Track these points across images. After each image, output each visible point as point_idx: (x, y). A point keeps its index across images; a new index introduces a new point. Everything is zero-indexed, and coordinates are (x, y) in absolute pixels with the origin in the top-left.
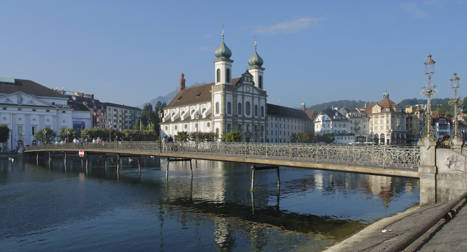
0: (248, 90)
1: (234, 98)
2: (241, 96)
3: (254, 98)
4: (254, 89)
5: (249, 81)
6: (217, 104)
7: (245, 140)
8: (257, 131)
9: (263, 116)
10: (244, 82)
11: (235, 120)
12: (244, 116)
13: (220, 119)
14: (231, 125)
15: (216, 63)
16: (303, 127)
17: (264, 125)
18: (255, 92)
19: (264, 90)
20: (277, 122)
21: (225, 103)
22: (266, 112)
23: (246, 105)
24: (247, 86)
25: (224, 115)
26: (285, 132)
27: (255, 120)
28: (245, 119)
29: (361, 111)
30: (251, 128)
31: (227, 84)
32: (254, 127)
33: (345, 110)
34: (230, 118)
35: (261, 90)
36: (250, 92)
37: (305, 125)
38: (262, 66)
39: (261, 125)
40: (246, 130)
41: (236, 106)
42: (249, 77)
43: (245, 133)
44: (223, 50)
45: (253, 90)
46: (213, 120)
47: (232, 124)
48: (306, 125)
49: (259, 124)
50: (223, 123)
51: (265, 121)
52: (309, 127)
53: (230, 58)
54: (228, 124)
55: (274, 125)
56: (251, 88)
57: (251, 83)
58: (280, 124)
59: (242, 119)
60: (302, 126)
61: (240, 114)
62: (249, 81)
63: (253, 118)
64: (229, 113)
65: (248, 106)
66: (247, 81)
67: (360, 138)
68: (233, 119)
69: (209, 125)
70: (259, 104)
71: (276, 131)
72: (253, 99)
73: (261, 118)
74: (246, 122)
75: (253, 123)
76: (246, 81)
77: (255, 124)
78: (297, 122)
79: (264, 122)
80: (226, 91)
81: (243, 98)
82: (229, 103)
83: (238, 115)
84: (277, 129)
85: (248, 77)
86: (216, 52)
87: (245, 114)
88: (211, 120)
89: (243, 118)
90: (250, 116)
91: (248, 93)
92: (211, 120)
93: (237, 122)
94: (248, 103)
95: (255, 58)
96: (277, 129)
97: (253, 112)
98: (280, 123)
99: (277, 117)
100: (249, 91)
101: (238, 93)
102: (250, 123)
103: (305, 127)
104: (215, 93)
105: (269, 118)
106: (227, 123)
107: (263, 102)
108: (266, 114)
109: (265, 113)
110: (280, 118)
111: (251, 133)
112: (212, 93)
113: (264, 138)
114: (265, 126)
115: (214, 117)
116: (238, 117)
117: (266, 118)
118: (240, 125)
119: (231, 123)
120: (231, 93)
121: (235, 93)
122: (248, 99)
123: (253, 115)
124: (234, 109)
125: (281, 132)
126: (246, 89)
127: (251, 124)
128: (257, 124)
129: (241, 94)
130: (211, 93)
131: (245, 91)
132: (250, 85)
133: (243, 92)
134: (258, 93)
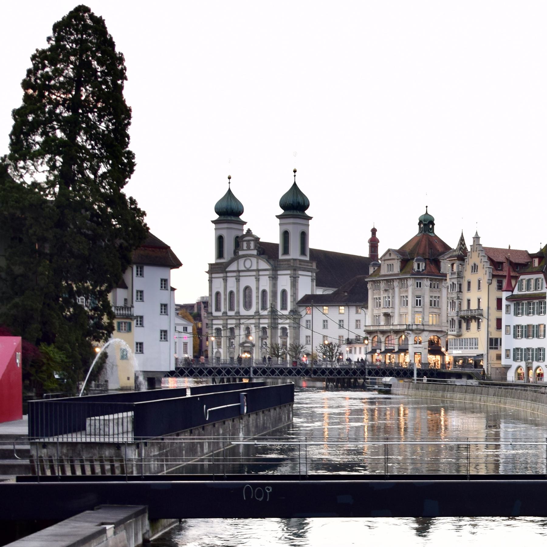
2: (234, 279)
4: (259, 260)
12: (238, 312)
14: (220, 329)
17: (287, 326)
36: (252, 268)
40: (243, 338)
43: (241, 342)
45: (257, 262)
56: (254, 260)
61: (231, 309)
66: (249, 248)
72: (258, 280)
75: (257, 326)
82: (218, 294)
85: (249, 241)
89: (239, 317)
90: (252, 312)
91: (248, 270)
97: (257, 303)
100: (250, 268)
101: (229, 274)
106: (212, 328)
114: (289, 327)
127: (253, 326)
128: (266, 326)
131: (242, 268)
133: (239, 271)
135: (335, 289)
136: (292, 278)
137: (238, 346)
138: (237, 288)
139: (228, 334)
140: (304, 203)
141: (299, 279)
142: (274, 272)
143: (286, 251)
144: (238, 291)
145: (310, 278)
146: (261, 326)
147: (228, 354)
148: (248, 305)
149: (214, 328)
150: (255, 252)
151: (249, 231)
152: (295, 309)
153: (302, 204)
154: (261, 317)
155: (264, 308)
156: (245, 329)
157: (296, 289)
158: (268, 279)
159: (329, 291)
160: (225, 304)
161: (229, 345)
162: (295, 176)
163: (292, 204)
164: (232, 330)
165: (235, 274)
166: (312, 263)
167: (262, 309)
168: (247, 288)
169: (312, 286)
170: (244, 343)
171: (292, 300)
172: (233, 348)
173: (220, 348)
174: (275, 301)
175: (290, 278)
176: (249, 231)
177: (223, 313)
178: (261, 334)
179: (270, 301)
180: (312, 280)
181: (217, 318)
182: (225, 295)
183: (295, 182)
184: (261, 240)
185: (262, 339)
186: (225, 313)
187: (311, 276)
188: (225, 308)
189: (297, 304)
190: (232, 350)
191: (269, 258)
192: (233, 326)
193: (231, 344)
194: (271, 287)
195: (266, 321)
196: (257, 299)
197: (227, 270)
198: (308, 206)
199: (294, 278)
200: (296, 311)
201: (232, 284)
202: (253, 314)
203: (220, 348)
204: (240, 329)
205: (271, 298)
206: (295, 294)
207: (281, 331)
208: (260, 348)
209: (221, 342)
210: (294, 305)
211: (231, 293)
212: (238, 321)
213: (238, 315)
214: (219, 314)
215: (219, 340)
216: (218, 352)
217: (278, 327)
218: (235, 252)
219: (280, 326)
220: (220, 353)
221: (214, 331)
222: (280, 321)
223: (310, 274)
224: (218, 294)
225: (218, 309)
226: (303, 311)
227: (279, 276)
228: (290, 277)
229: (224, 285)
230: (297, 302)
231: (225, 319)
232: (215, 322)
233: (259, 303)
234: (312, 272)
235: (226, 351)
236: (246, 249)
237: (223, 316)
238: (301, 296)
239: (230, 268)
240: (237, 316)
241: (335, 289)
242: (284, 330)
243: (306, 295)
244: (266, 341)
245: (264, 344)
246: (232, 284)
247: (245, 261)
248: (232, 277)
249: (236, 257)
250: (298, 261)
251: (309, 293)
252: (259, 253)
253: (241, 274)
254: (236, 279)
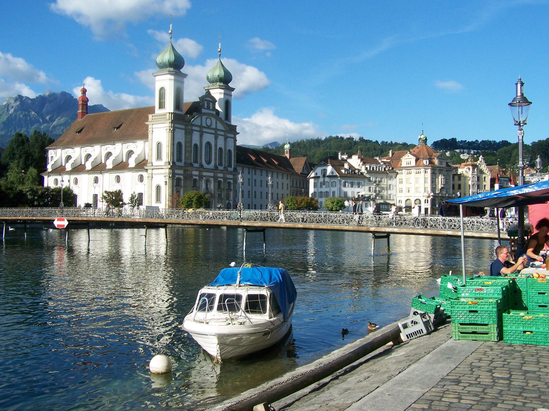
0: (209, 124)
1: (188, 136)
2: (198, 133)
3: (218, 137)
5: (211, 108)
6: (159, 145)
8: (222, 191)
9: (230, 166)
10: (204, 111)
11: (189, 173)
12: (201, 166)
14: (181, 179)
15: (158, 78)
16: (289, 185)
17: (232, 181)
18: (220, 126)
19: (233, 123)
20: (250, 176)
21: (173, 144)
22: (236, 160)
23: (205, 148)
25: (171, 164)
26: (261, 192)
27: (219, 173)
28: (204, 171)
29: (385, 163)
30: (212, 186)
31: (177, 112)
32: (217, 184)
33: (359, 160)
34: (180, 168)
35: (228, 123)
36: (211, 127)
37: (291, 182)
38: (230, 85)
41: (189, 149)
42: (211, 102)
44: (172, 56)
45: (216, 123)
46: (150, 171)
47: (182, 178)
48: (293, 181)
49: (225, 179)
50: (170, 177)
51: (234, 175)
52: (298, 185)
53: (181, 70)
56: (214, 120)
58: (255, 180)
59: (200, 171)
60: (287, 184)
61: (196, 162)
62: (211, 108)
64: (179, 160)
65: (208, 150)
66: (208, 108)
67: (384, 206)
68: (185, 171)
69: (141, 179)
70: (225, 146)
71: (249, 192)
72: (216, 138)
73: (227, 170)
74: (205, 176)
75: (215, 178)
76: (205, 109)
77: (219, 179)
78: (280, 177)
79: (231, 176)
81: (201, 136)
82: (179, 144)
84: (249, 188)
85: (208, 101)
86: (159, 59)
87: (204, 163)
88: (147, 170)
91: (209, 127)
92: (147, 170)
93: (191, 176)
95: (220, 71)
96: (249, 188)
98: (254, 177)
99: (251, 168)
101: (194, 128)
102: (211, 177)
103: (292, 185)
104: (154, 126)
105: (240, 170)
107: (230, 142)
108: (235, 163)
109: (234, 161)
110: (255, 170)
112: (150, 127)
113: (231, 202)
115: (152, 166)
116: (193, 167)
117: (235, 169)
118: (195, 180)
119: (182, 177)
120: (183, 127)
121: (190, 127)
122: (208, 138)
123: (215, 163)
124: (187, 153)
125: (255, 192)
126: (206, 121)
127: (212, 179)
128: (222, 180)
129: (198, 129)
130: (147, 126)
131: (204, 125)
132: (212, 115)
133: (201, 126)
168: (208, 144)
246: (196, 138)
247: (207, 118)
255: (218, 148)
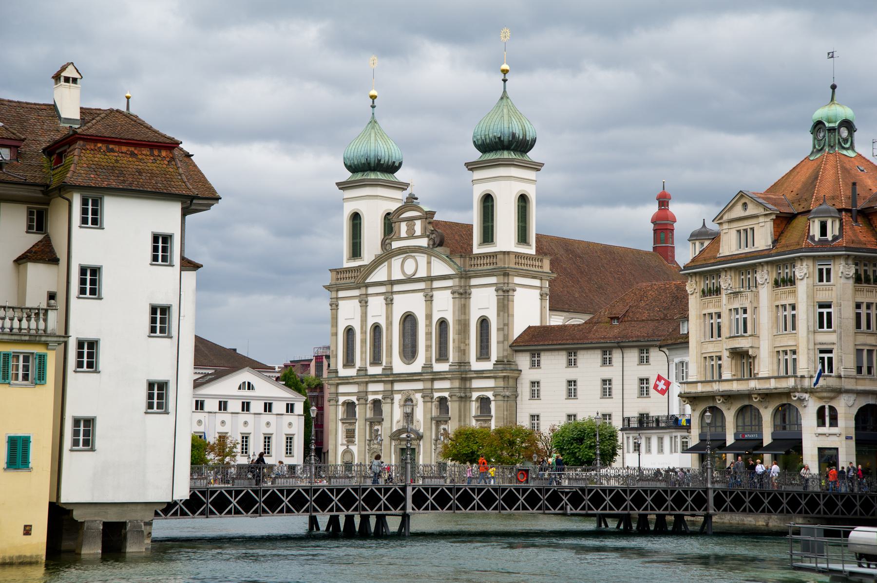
2: (381, 298)
4: (433, 258)
7: (393, 456)
13: (357, 386)
14: (353, 403)
17: (490, 394)
24: (404, 255)
39: (475, 395)
45: (429, 263)
54: (344, 403)
55: (589, 388)
56: (422, 259)
57: (424, 242)
63: (429, 375)
66: (411, 236)
72: (429, 299)
74: (399, 391)
75: (427, 395)
80: (337, 291)
81: (389, 302)
82: (350, 331)
83: (366, 370)
89: (390, 378)
91: (410, 280)
94: (409, 319)
97: (428, 347)
101: (371, 290)
106: (337, 401)
111: (421, 431)
114: (495, 396)
121: (363, 291)
123: (428, 359)
127: (418, 396)
128: (446, 394)
131: (397, 275)
132: (418, 250)
133: (392, 283)
134: (452, 272)
135: (587, 317)
136: (501, 293)
137: (389, 439)
138: (387, 318)
139: (369, 414)
140: (525, 135)
141: (515, 293)
142: (463, 280)
143: (488, 236)
144: (390, 324)
145: (538, 292)
146: (436, 395)
147: (367, 455)
148: (409, 352)
149: (340, 402)
150: (424, 242)
151: (412, 198)
152: (507, 357)
153: (521, 137)
154: (438, 376)
155: (442, 356)
156: (402, 403)
157: (508, 316)
158: (451, 296)
159: (578, 320)
160: (363, 352)
161: (371, 436)
162: (505, 81)
163: (500, 138)
164: (377, 404)
165: (382, 289)
166: (541, 260)
167: (438, 360)
168: (409, 319)
169: (542, 308)
170: (400, 432)
171: (501, 339)
172: (378, 443)
173: (353, 442)
174: (465, 343)
175: (495, 293)
176: (412, 198)
177: (358, 370)
178: (435, 412)
179: (454, 342)
180: (541, 295)
181: (346, 381)
182: (364, 332)
183: (505, 91)
184: (437, 217)
185: (438, 423)
186: (363, 370)
187: (541, 288)
188: (363, 359)
189: (510, 346)
190: (376, 446)
191: (453, 252)
192: (380, 397)
193: (375, 435)
194: (457, 313)
195: (446, 384)
196: (427, 340)
197: (367, 281)
198: (534, 141)
199: (504, 291)
200: (509, 362)
201: (377, 309)
202: (419, 370)
203: (353, 442)
204: (392, 403)
205: (457, 337)
206: (505, 327)
207: (478, 404)
208: (433, 442)
209: (354, 430)
210: (504, 350)
211: (377, 328)
212: (388, 387)
213: (389, 372)
214: (351, 372)
215: (351, 427)
216: (347, 452)
217: (471, 397)
218: (384, 244)
219: (475, 395)
220: (352, 455)
221: (341, 410)
222: (476, 384)
223: (537, 283)
224: (350, 331)
225: (349, 362)
226: (523, 361)
227: (473, 290)
228: (497, 290)
229: (362, 313)
230: (511, 342)
231: (362, 382)
232: (342, 389)
233: (431, 346)
234: (541, 279)
235: (363, 449)
236: (406, 236)
237: (358, 376)
238: (518, 330)
239: (374, 278)
240: (387, 375)
241: (587, 317)
242: (484, 402)
243: (529, 327)
244: (446, 427)
245: (442, 435)
246: (377, 309)
248: (377, 294)
249: (387, 255)
250: (512, 256)
251: (537, 323)
252: (431, 243)
253: (396, 288)
254: (386, 299)
255: (435, 319)
